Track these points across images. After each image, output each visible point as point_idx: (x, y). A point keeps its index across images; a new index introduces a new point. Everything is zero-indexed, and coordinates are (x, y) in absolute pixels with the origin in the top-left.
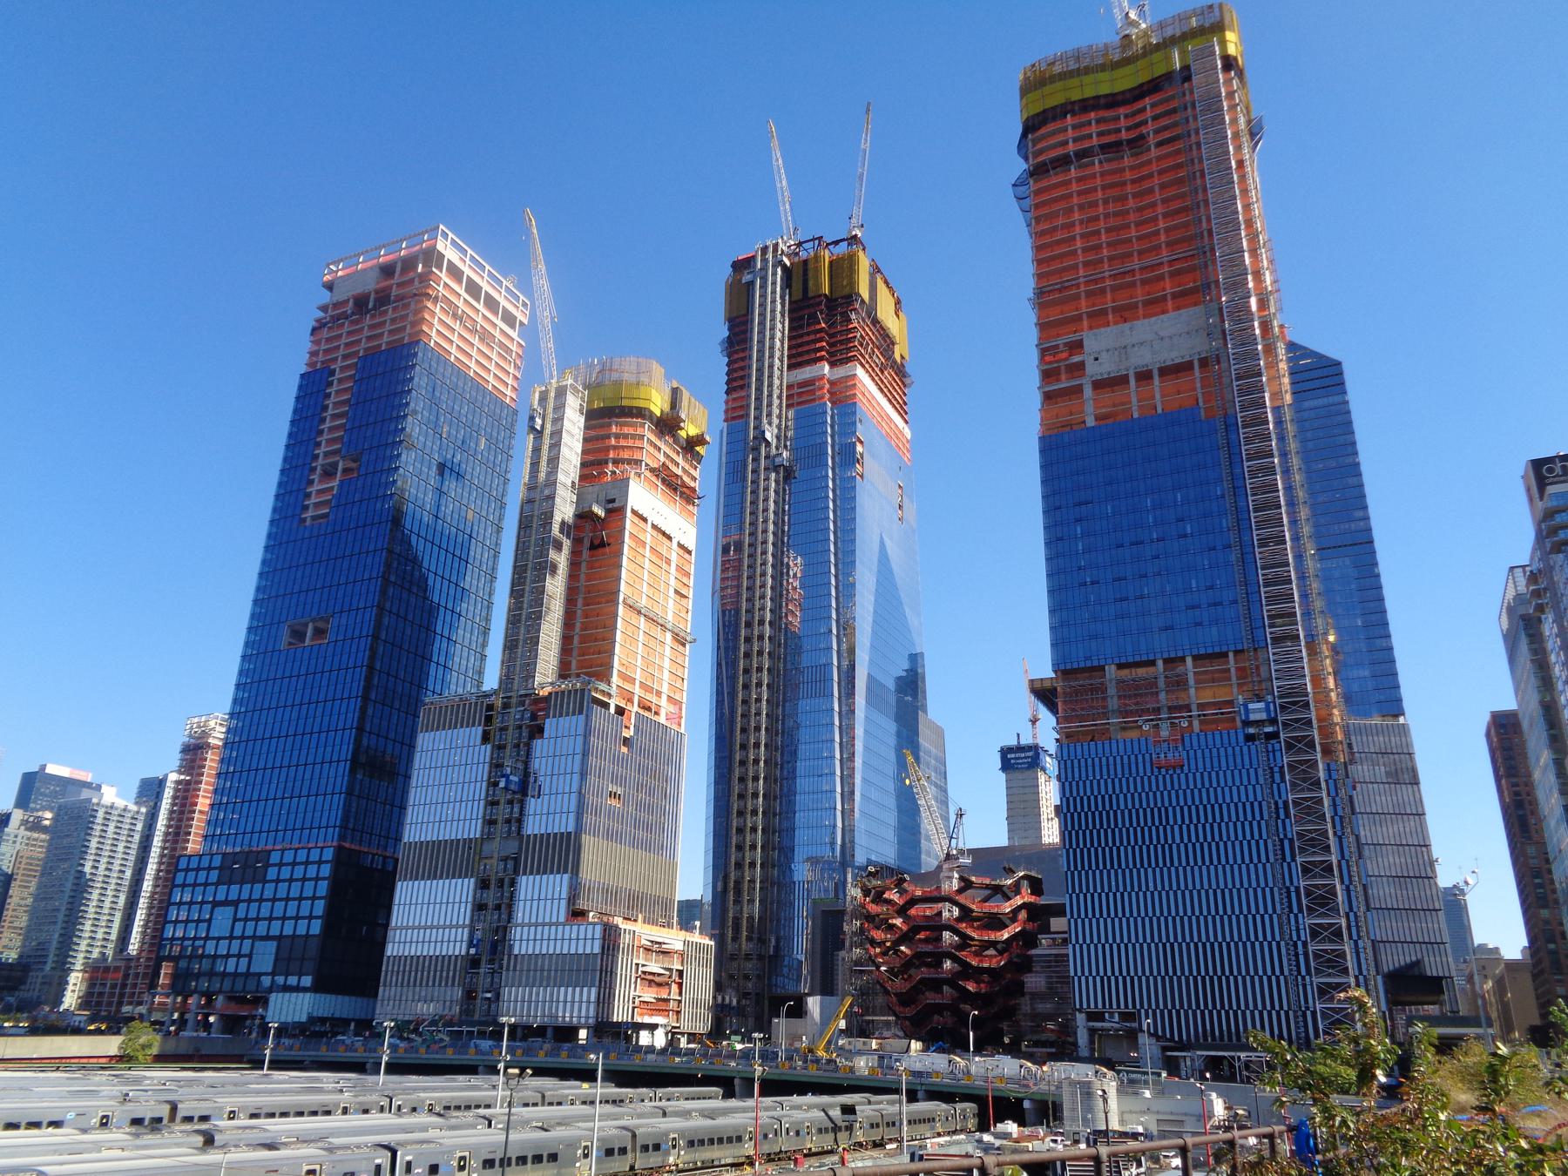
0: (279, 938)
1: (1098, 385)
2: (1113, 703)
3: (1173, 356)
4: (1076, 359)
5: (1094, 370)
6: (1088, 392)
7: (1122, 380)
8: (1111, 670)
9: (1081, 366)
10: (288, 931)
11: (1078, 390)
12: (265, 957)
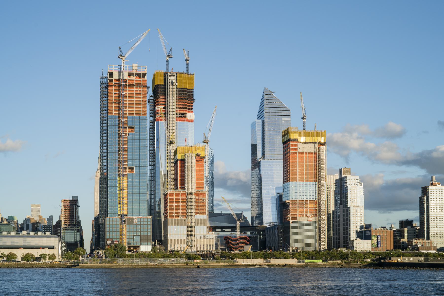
0: (140, 236)
1: (299, 153)
2: (298, 206)
3: (311, 151)
4: (296, 147)
5: (299, 151)
6: (298, 153)
7: (302, 153)
8: (298, 201)
9: (296, 149)
10: (142, 234)
11: (296, 153)
12: (137, 239)
